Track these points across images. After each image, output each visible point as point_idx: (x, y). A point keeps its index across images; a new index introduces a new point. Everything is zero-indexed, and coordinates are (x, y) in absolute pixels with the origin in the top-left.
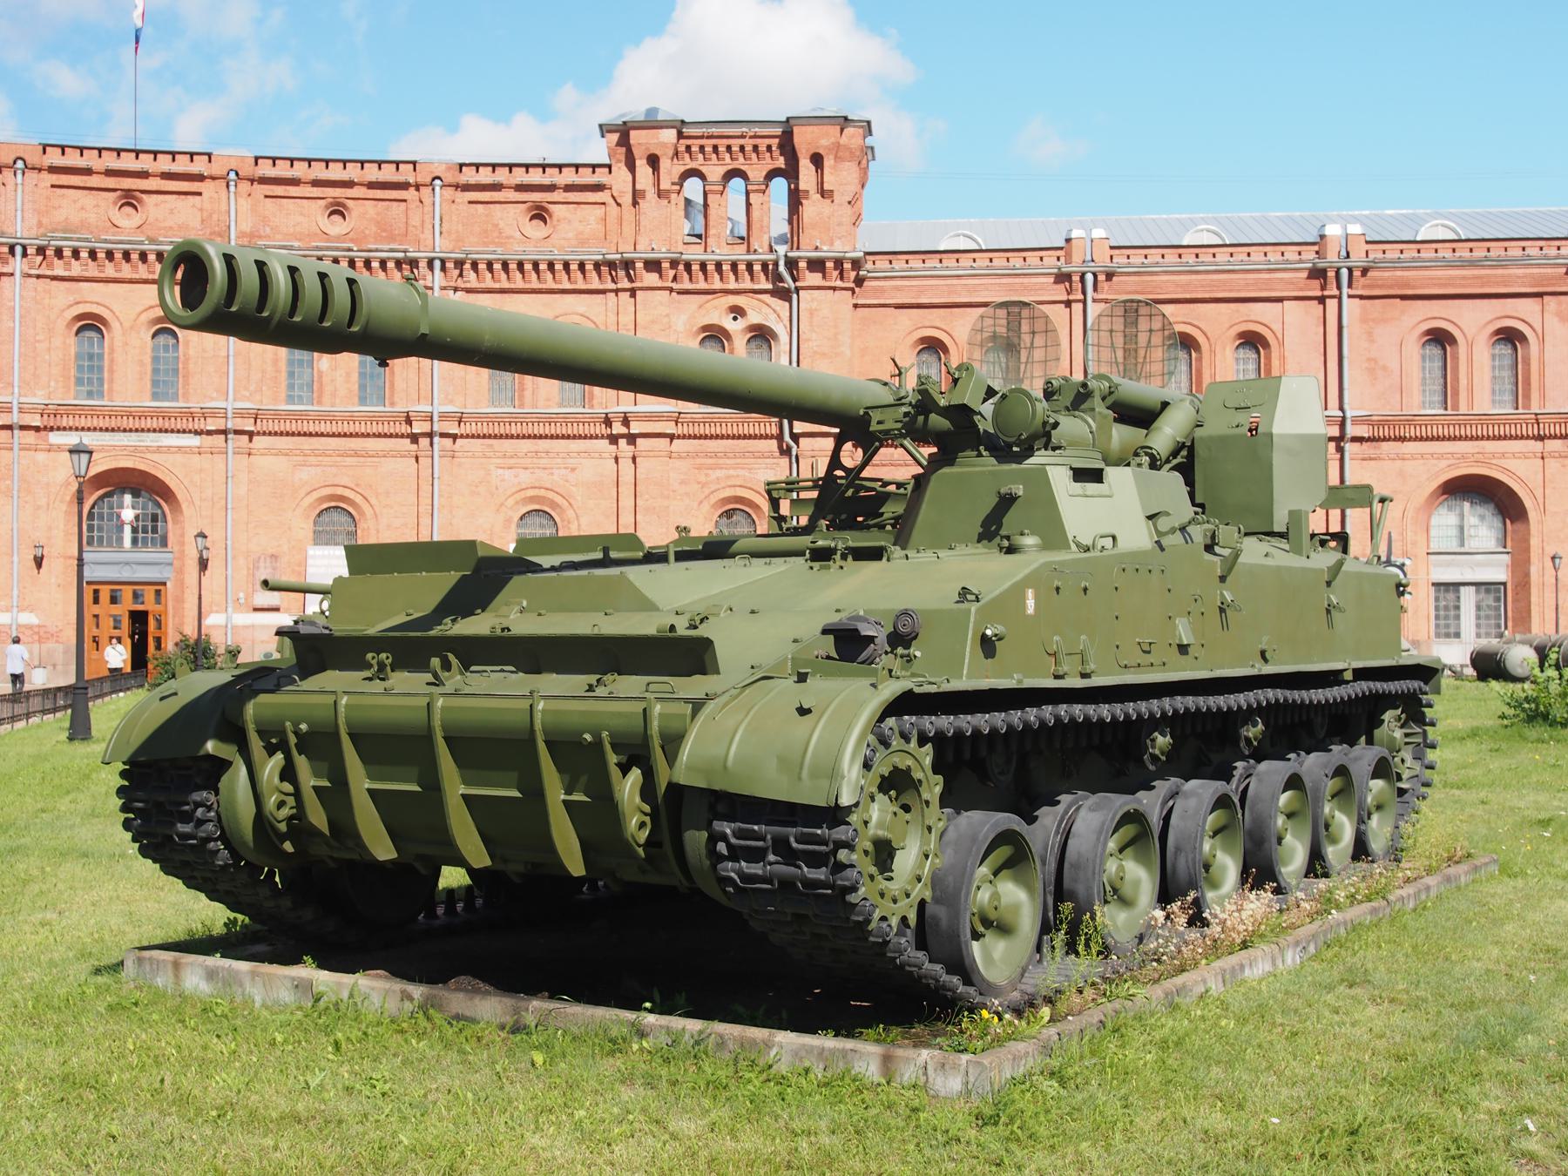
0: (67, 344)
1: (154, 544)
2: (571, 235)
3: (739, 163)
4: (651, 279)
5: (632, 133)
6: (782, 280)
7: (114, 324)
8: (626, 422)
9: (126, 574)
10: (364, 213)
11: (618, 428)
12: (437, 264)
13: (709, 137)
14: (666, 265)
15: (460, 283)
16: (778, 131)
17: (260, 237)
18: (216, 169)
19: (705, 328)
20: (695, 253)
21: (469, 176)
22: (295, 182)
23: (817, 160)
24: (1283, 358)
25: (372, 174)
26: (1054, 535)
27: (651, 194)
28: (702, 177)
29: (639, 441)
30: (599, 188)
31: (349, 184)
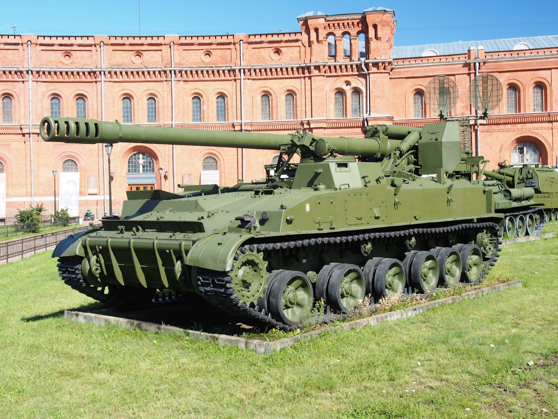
0: (120, 104)
1: (150, 171)
2: (288, 58)
3: (347, 29)
4: (316, 72)
5: (309, 21)
6: (363, 71)
8: (308, 123)
9: (141, 182)
10: (217, 54)
11: (306, 126)
12: (242, 71)
13: (336, 20)
14: (322, 67)
15: (250, 77)
16: (360, 17)
17: (182, 64)
18: (167, 41)
19: (337, 89)
20: (332, 62)
21: (252, 39)
22: (192, 44)
23: (375, 26)
24: (551, 91)
26: (330, 184)
27: (315, 42)
28: (334, 35)
29: (314, 130)
30: (297, 41)
31: (211, 44)
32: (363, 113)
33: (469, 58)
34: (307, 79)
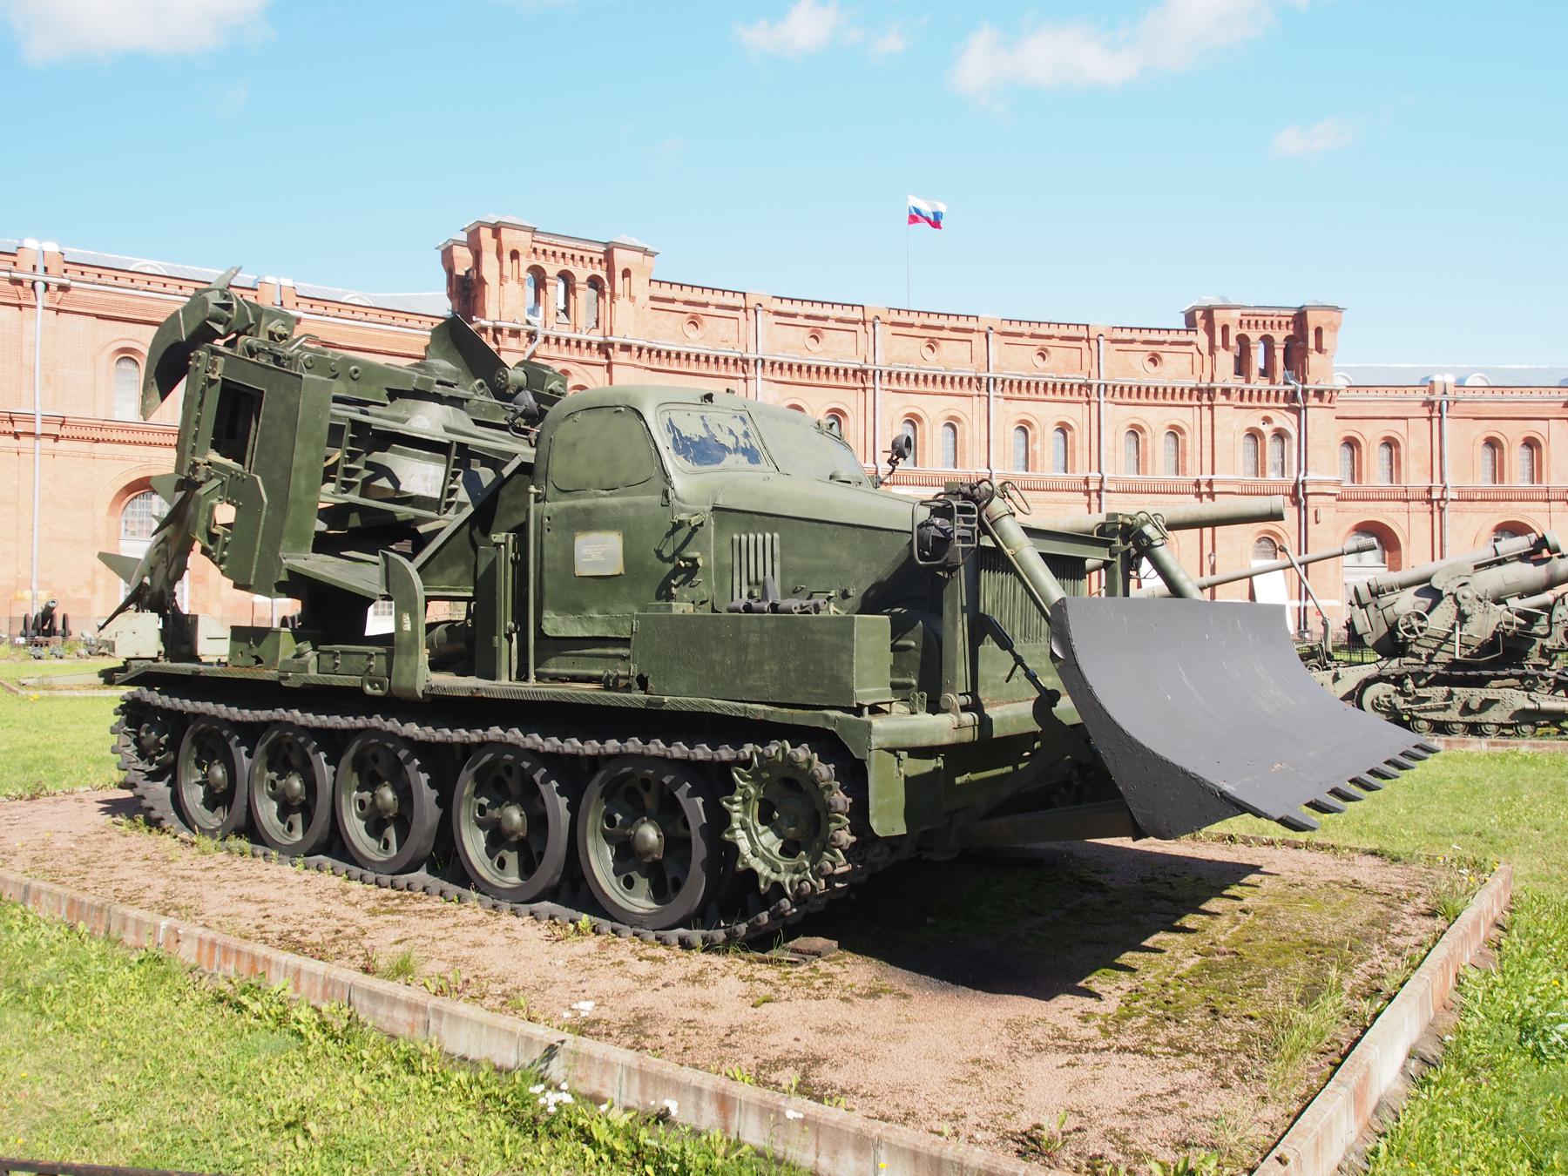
5: (1216, 312)
7: (926, 420)
8: (1210, 484)
10: (1058, 354)
22: (1021, 335)
23: (1319, 331)
25: (1064, 331)
30: (1189, 343)
32: (1290, 471)
33: (1432, 391)
34: (1205, 409)
